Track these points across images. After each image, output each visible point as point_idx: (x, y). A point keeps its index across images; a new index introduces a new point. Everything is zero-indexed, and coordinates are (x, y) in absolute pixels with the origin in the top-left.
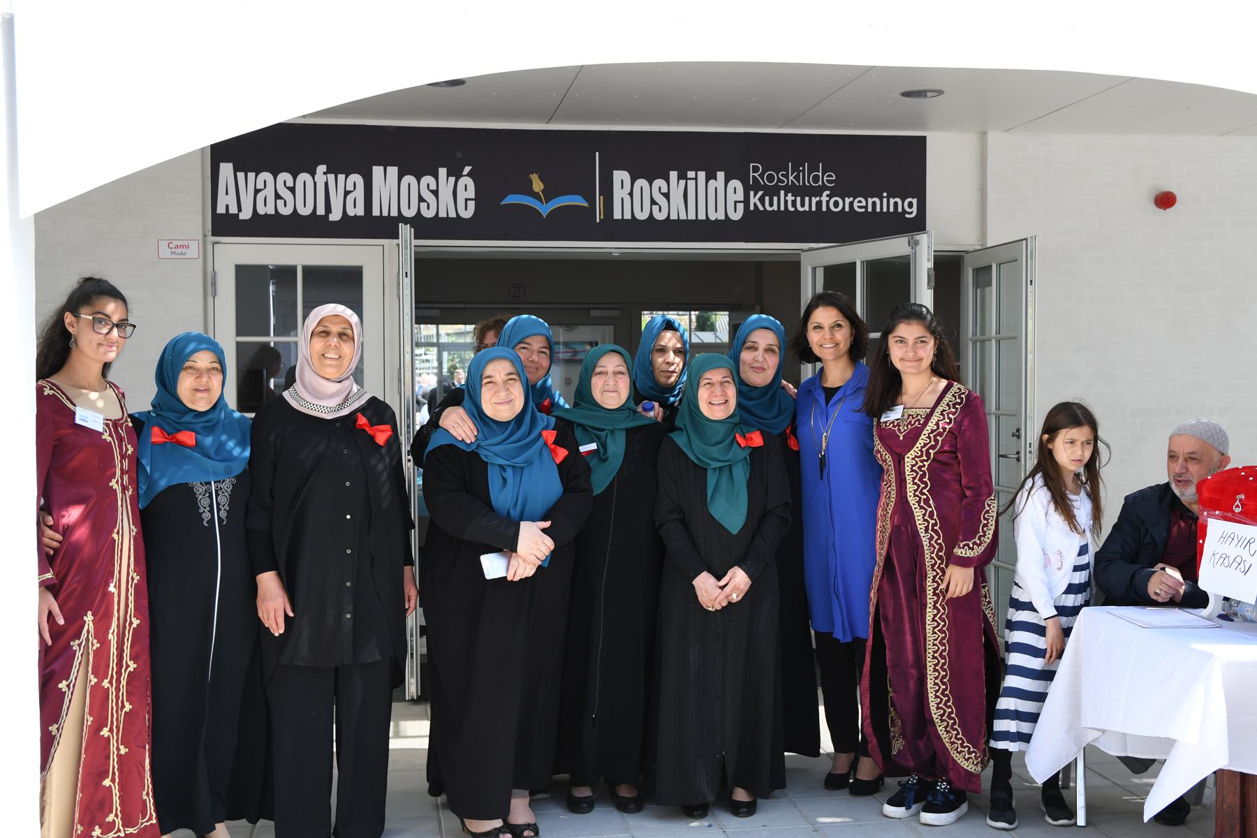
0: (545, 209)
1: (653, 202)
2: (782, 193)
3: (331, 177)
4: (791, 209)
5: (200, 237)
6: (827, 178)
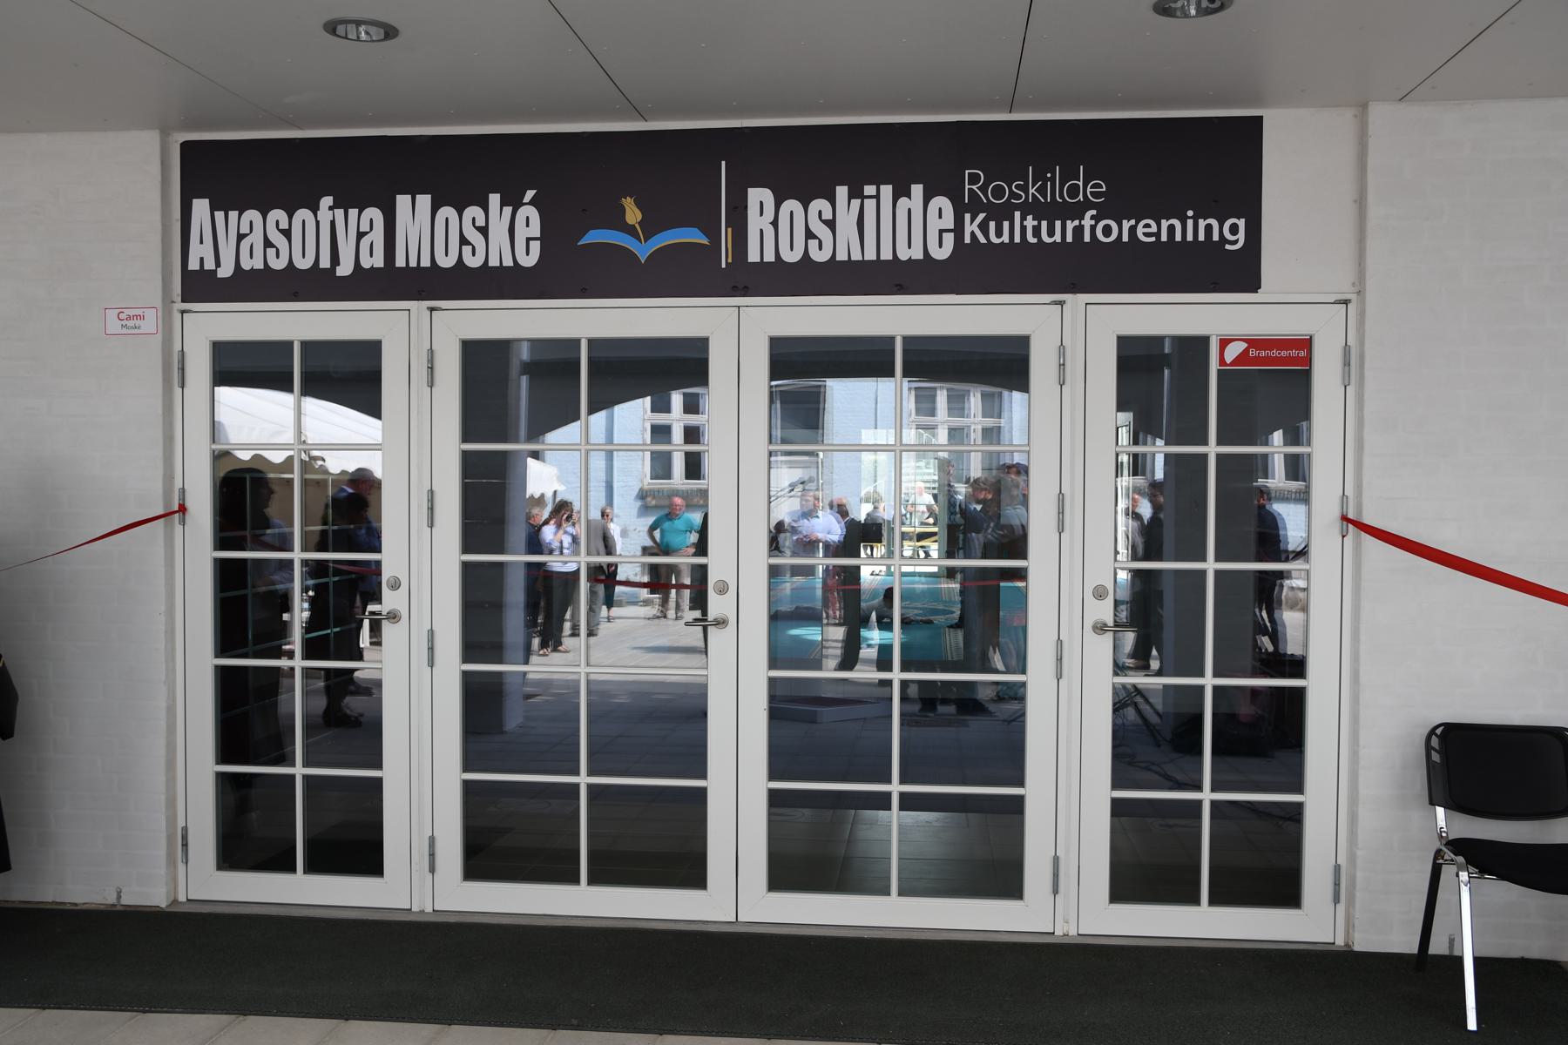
0: (643, 250)
2: (1017, 214)
3: (339, 213)
4: (1031, 239)
5: (158, 303)
6: (1091, 189)
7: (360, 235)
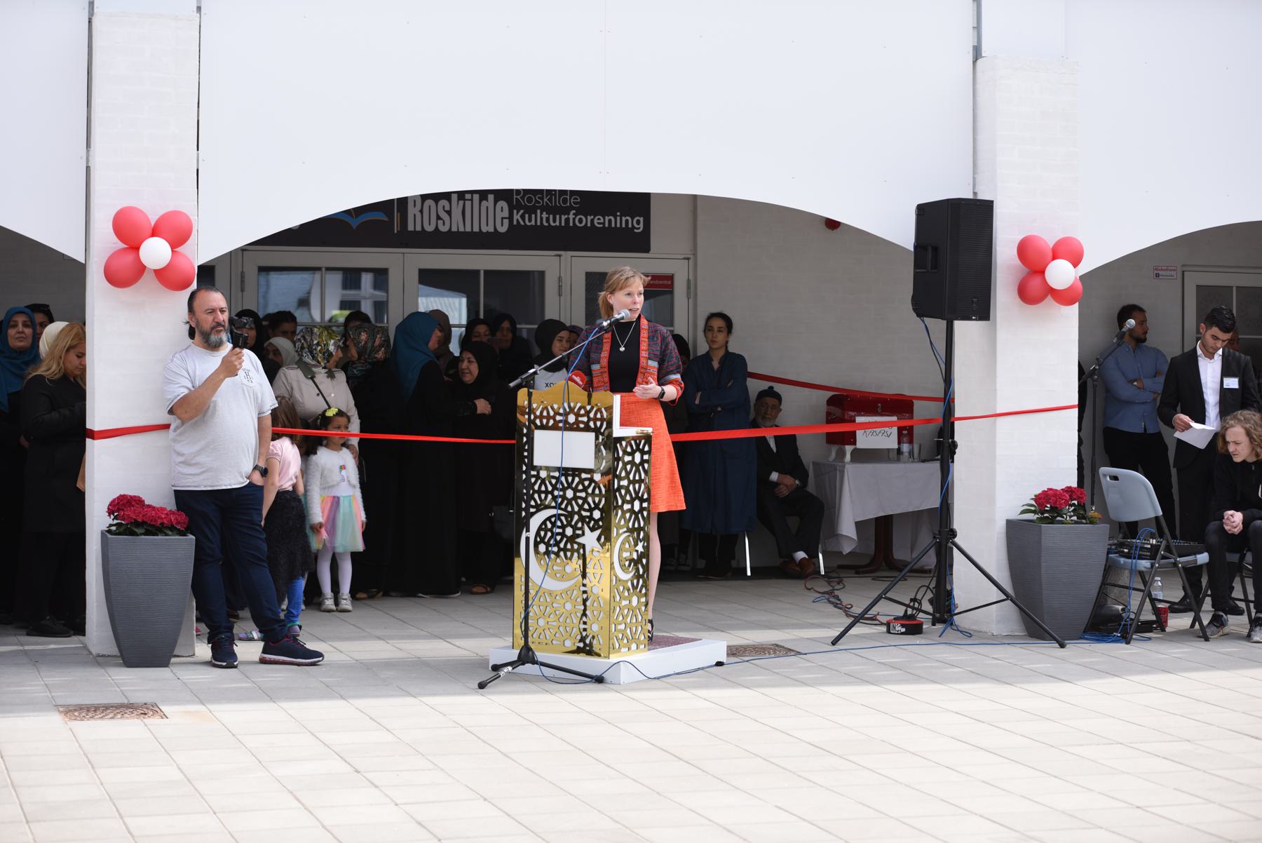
1: (439, 218)
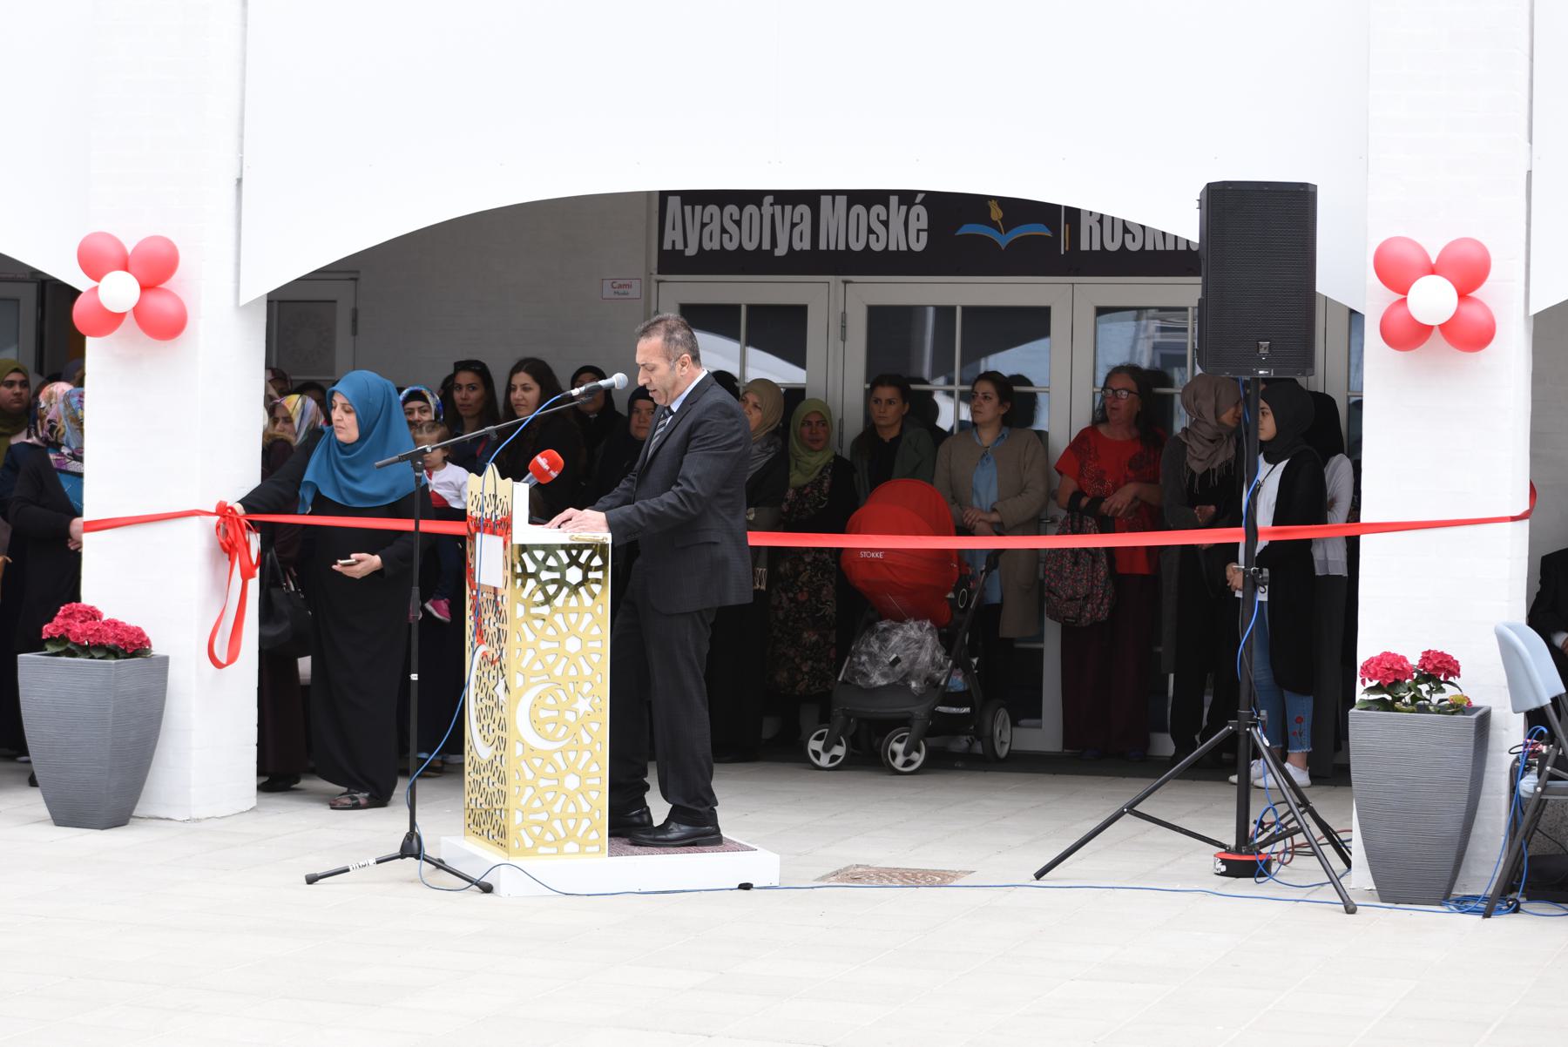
0: (1003, 240)
3: (778, 208)
7: (793, 225)
